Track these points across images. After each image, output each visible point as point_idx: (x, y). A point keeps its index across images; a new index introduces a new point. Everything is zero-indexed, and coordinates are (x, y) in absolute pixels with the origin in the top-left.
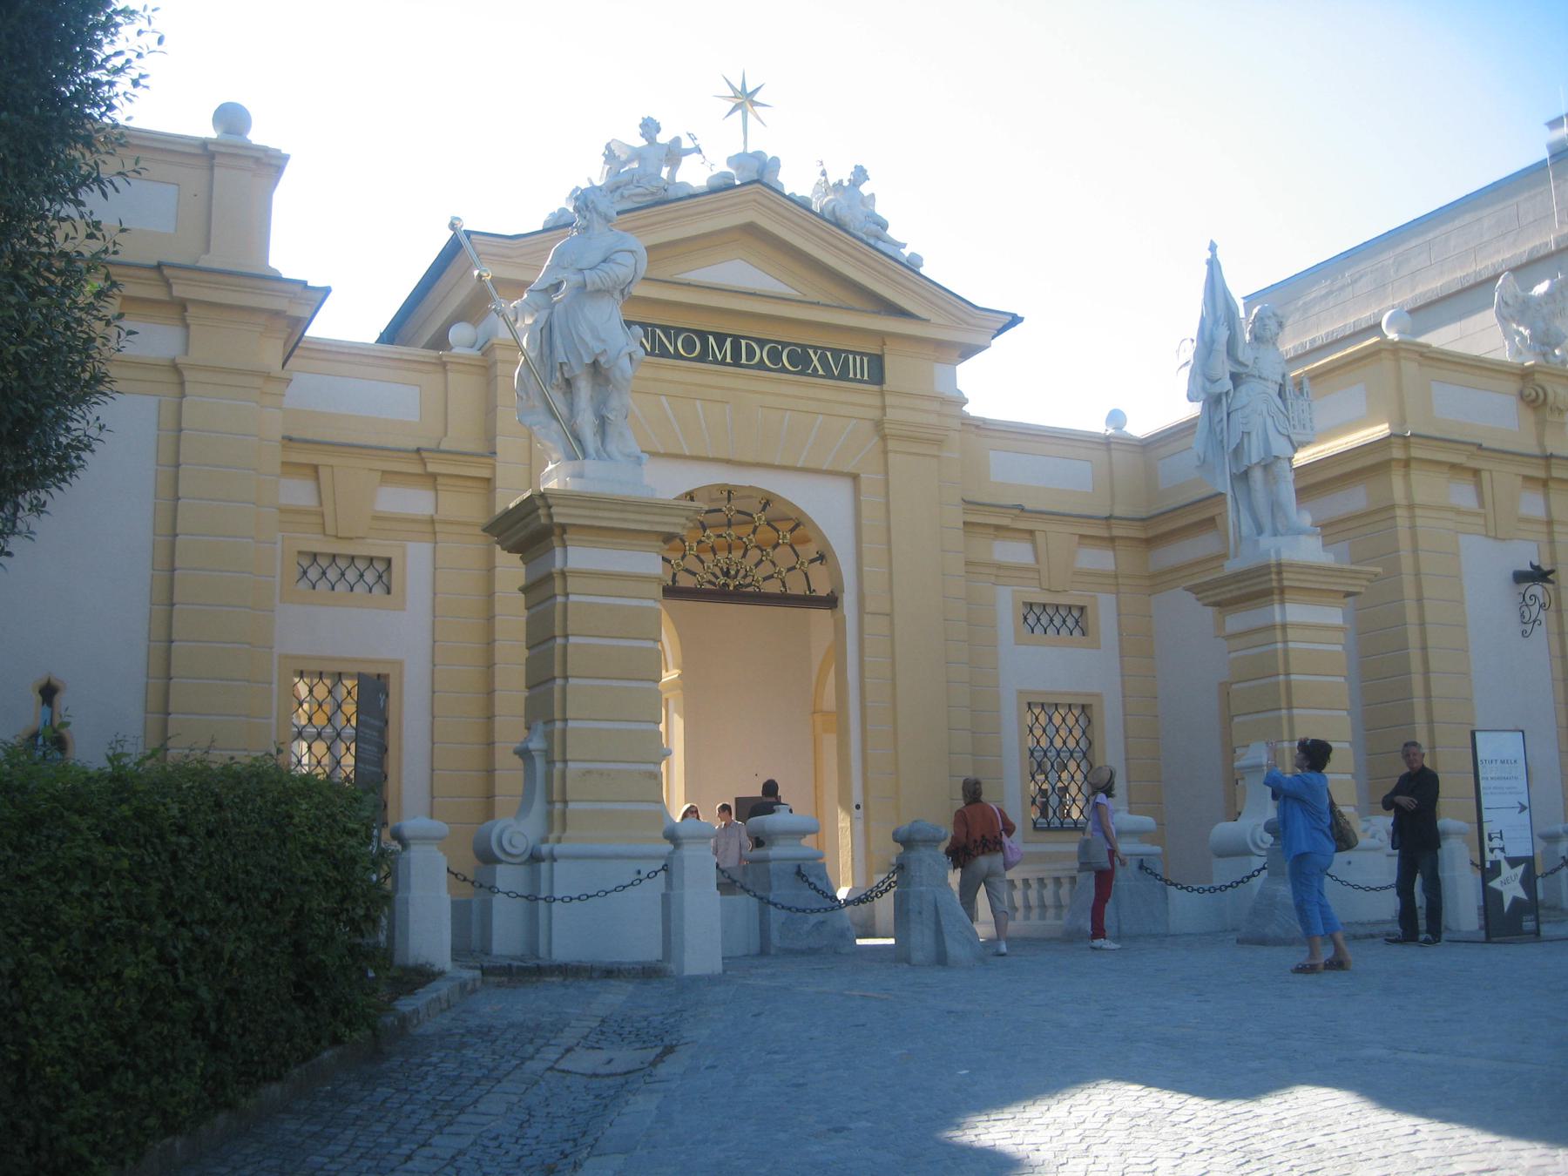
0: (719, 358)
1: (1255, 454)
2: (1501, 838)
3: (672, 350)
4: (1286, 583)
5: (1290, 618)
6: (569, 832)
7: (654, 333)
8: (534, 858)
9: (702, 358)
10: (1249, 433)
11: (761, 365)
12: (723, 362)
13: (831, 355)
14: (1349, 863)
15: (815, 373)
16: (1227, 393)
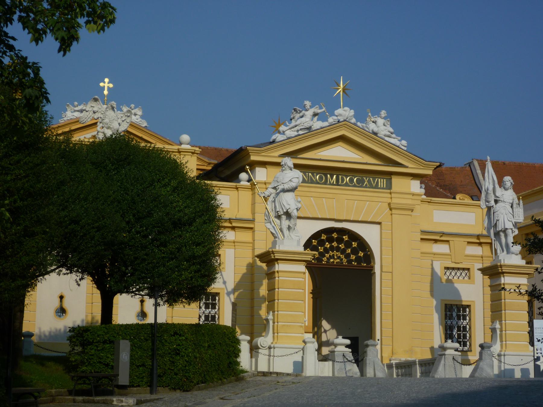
0: (332, 182)
1: (500, 227)
2: (541, 350)
3: (314, 180)
4: (504, 271)
5: (506, 282)
6: (278, 341)
7: (308, 175)
8: (270, 348)
9: (325, 183)
10: (498, 220)
11: (347, 185)
12: (333, 184)
13: (372, 179)
14: (522, 360)
15: (366, 187)
16: (493, 206)
